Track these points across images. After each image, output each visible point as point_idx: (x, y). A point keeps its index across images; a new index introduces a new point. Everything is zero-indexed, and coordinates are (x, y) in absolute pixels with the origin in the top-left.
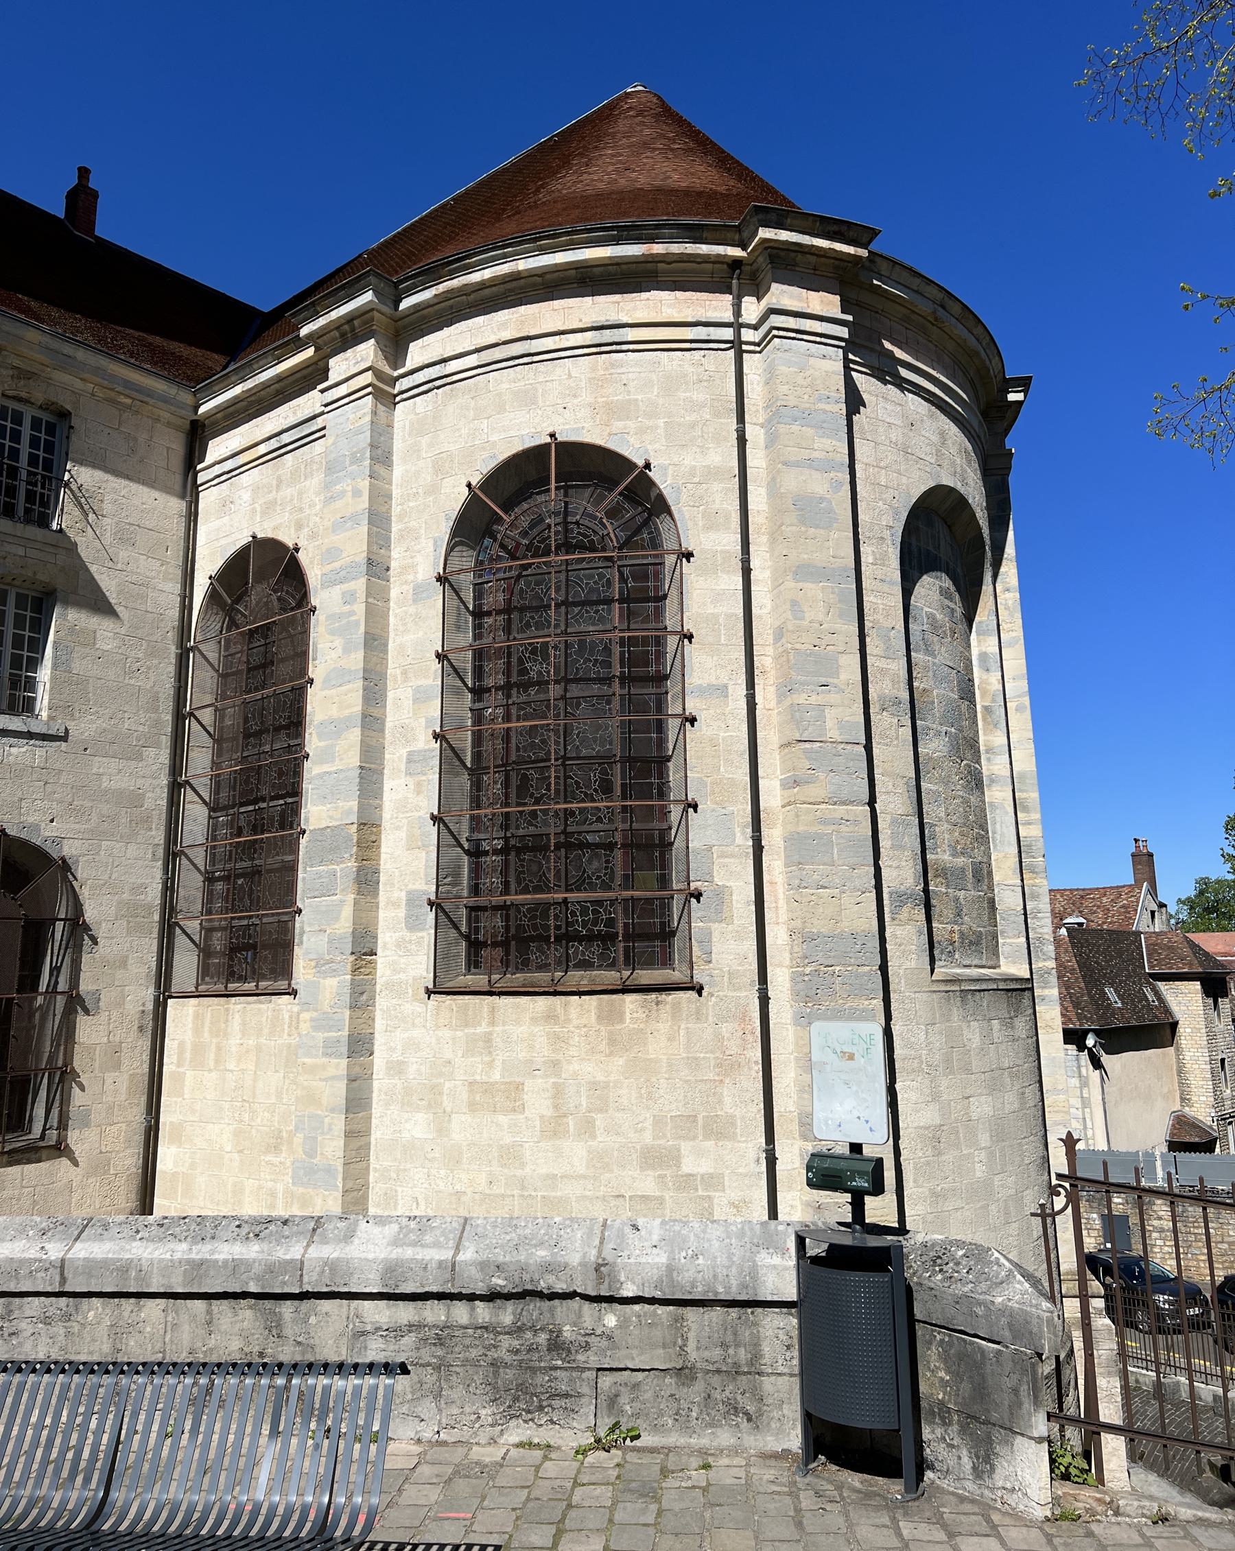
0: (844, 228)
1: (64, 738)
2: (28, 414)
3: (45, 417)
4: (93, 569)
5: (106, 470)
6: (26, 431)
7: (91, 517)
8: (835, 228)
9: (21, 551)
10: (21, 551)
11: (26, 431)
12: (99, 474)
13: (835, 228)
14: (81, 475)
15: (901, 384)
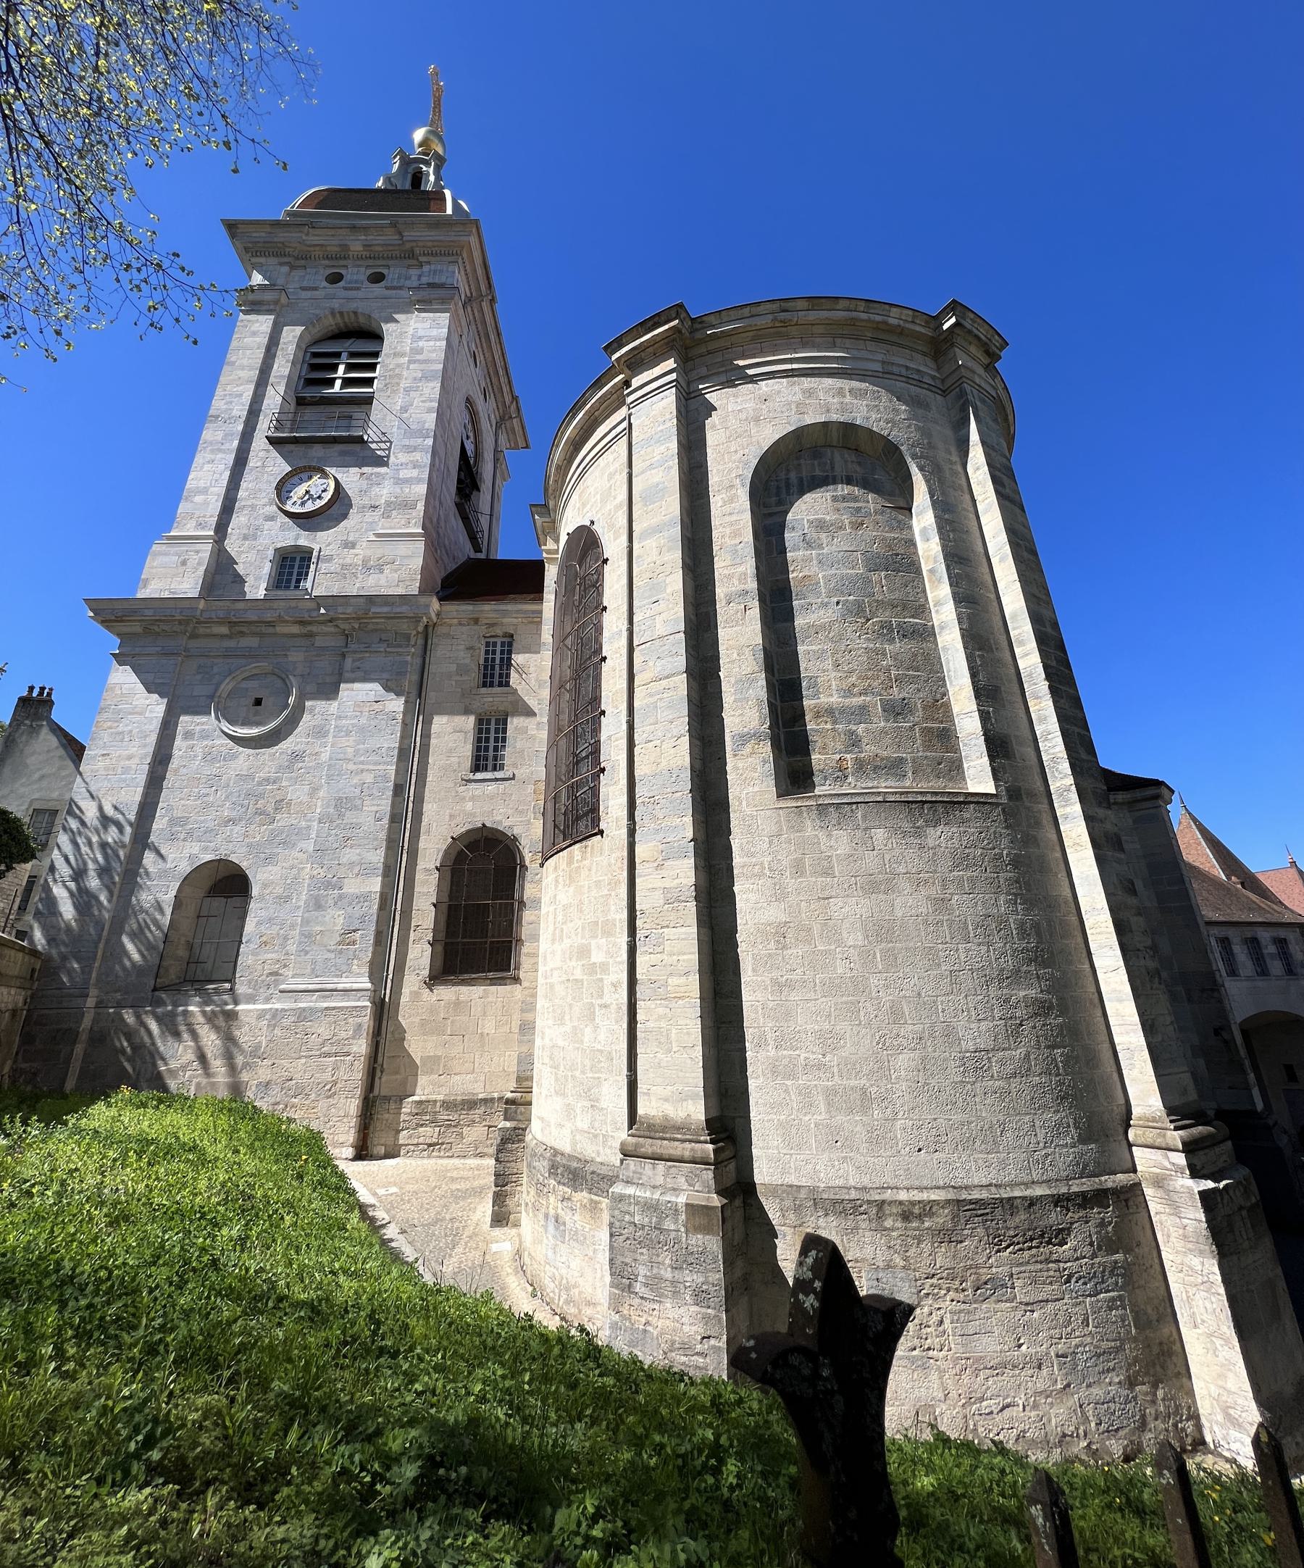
0: (656, 319)
1: (513, 778)
2: (499, 641)
3: (506, 640)
4: (526, 699)
5: (531, 653)
6: (498, 648)
7: (524, 676)
8: (651, 323)
9: (491, 699)
10: (491, 699)
11: (498, 648)
12: (527, 655)
13: (651, 323)
14: (518, 659)
15: (752, 380)
